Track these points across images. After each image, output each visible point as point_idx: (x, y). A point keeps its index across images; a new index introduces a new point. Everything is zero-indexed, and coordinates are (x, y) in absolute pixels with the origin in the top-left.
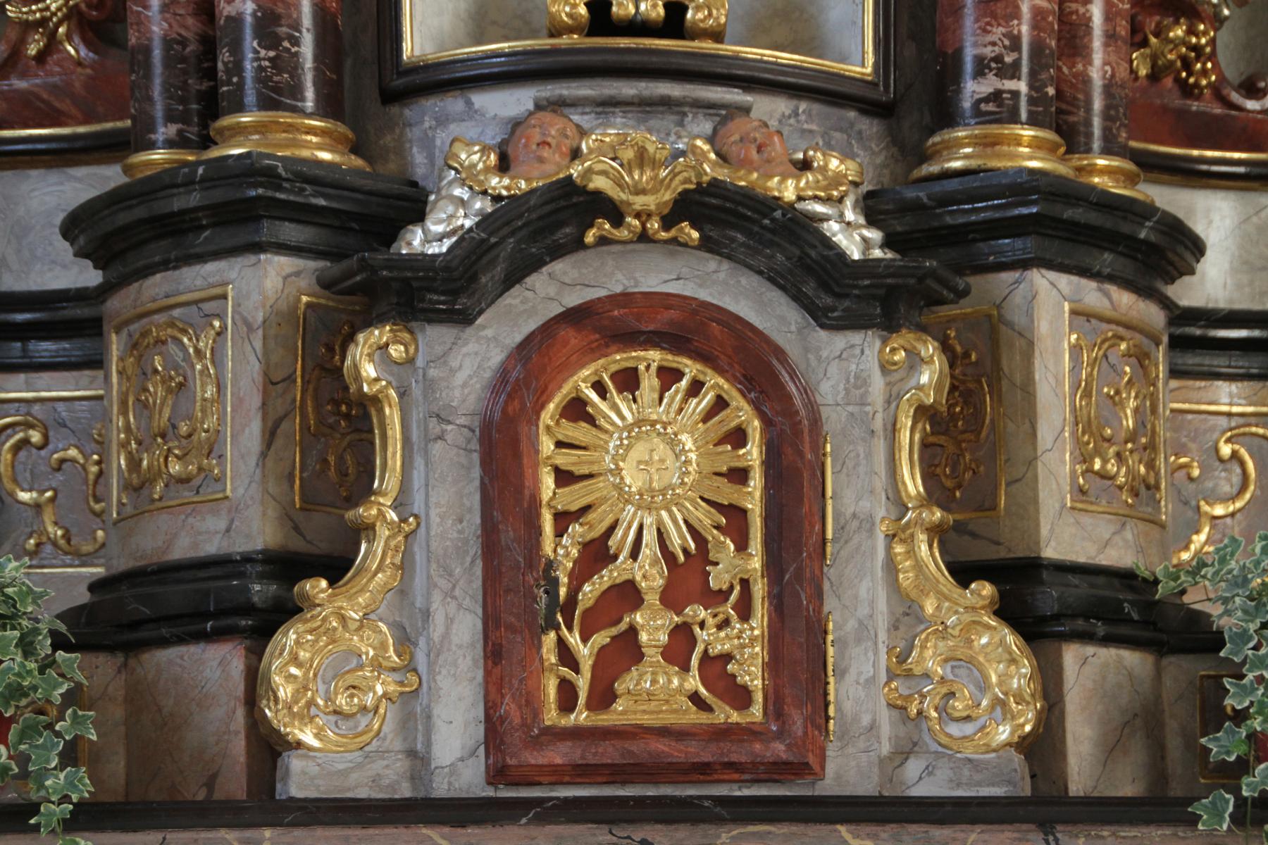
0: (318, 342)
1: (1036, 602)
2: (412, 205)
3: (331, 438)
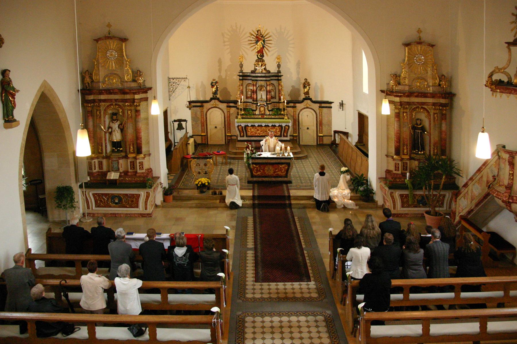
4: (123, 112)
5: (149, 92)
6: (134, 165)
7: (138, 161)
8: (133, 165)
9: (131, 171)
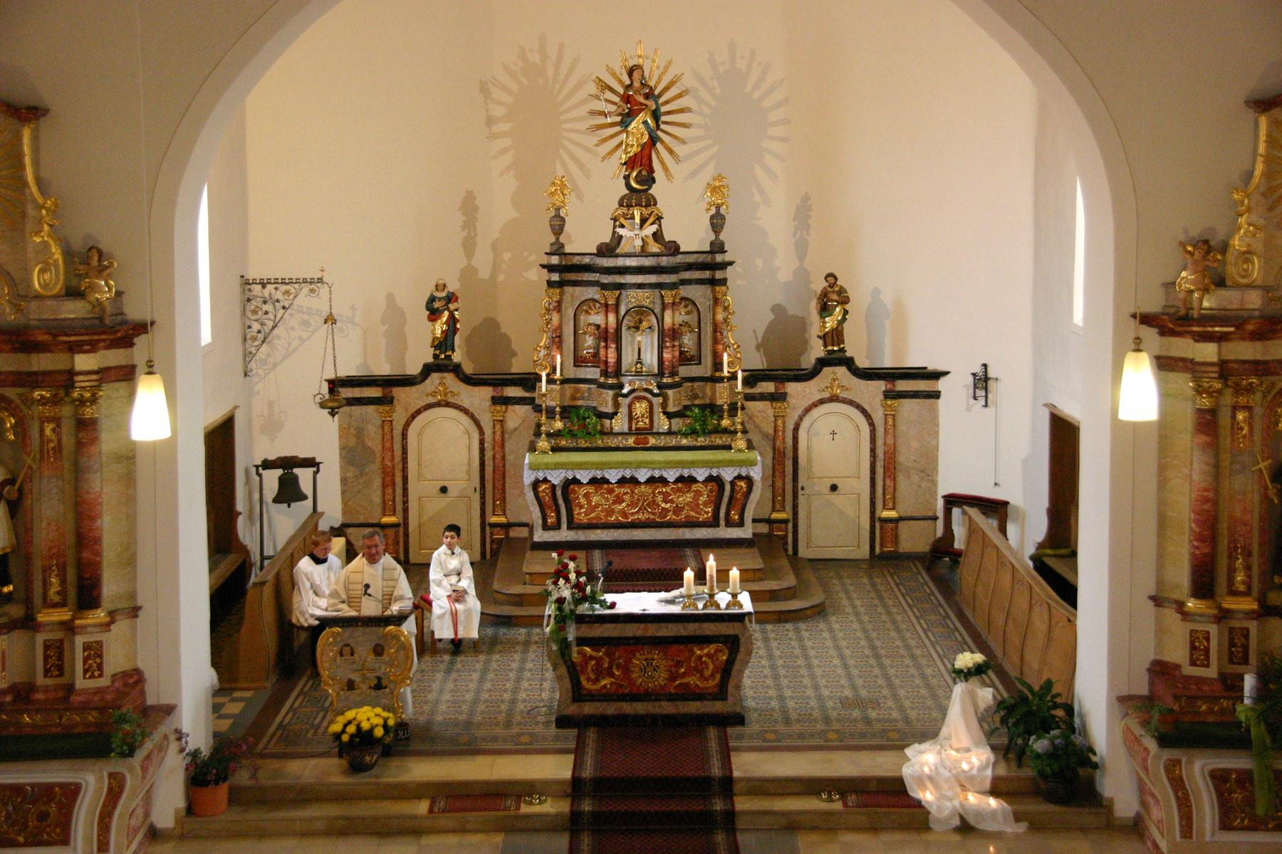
0: (615, 397)
1: (670, 416)
2: (621, 386)
3: (617, 405)
4: (21, 428)
5: (140, 341)
6: (60, 657)
7: (80, 640)
8: (56, 657)
9: (50, 682)
